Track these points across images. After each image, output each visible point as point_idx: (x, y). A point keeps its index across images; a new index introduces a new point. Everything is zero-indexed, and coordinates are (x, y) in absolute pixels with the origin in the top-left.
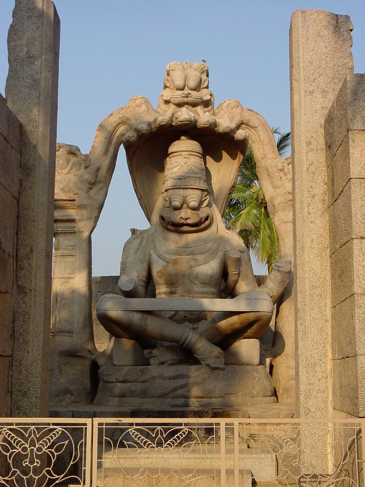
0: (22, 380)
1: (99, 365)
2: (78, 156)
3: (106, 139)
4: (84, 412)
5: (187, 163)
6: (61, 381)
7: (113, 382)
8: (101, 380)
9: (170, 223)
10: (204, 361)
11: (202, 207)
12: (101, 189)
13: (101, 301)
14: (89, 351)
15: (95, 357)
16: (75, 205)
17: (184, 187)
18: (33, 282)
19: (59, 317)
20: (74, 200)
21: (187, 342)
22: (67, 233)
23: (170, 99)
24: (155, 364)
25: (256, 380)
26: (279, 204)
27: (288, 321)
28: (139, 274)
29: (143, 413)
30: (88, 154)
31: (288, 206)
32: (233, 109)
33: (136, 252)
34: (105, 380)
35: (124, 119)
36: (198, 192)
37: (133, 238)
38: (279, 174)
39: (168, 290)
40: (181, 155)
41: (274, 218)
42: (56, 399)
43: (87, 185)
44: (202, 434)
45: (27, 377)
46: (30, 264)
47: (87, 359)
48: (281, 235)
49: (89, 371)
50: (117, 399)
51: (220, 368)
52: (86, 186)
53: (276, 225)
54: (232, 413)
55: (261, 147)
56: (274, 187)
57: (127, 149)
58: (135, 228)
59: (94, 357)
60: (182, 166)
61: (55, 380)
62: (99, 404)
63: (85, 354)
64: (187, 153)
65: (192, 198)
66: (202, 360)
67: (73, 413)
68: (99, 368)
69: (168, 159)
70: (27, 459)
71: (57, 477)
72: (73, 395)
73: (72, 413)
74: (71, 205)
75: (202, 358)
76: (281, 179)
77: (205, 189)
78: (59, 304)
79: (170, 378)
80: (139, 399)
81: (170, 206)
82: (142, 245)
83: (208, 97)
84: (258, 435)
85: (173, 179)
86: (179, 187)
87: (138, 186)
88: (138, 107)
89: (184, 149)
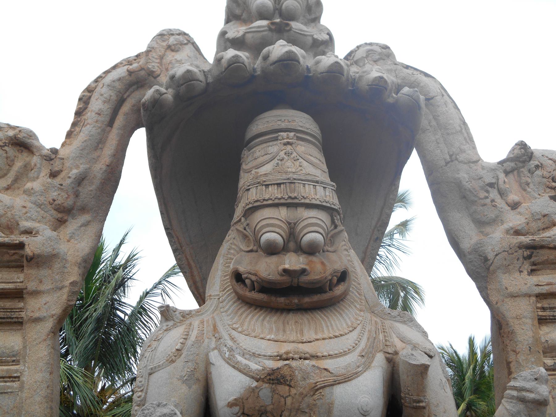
2: (35, 150)
9: (255, 283)
11: (330, 249)
12: (86, 224)
16: (23, 256)
17: (290, 201)
20: (21, 246)
23: (244, 35)
26: (497, 255)
30: (58, 147)
31: (518, 259)
35: (143, 73)
36: (323, 216)
37: (165, 328)
38: (487, 195)
40: (277, 140)
41: (487, 288)
43: (54, 212)
48: (508, 324)
52: (52, 216)
53: (494, 303)
60: (281, 160)
64: (292, 134)
69: (245, 152)
74: (13, 258)
76: (493, 203)
77: (336, 208)
81: (255, 248)
82: (189, 342)
85: (263, 185)
88: (173, 51)
89: (283, 125)
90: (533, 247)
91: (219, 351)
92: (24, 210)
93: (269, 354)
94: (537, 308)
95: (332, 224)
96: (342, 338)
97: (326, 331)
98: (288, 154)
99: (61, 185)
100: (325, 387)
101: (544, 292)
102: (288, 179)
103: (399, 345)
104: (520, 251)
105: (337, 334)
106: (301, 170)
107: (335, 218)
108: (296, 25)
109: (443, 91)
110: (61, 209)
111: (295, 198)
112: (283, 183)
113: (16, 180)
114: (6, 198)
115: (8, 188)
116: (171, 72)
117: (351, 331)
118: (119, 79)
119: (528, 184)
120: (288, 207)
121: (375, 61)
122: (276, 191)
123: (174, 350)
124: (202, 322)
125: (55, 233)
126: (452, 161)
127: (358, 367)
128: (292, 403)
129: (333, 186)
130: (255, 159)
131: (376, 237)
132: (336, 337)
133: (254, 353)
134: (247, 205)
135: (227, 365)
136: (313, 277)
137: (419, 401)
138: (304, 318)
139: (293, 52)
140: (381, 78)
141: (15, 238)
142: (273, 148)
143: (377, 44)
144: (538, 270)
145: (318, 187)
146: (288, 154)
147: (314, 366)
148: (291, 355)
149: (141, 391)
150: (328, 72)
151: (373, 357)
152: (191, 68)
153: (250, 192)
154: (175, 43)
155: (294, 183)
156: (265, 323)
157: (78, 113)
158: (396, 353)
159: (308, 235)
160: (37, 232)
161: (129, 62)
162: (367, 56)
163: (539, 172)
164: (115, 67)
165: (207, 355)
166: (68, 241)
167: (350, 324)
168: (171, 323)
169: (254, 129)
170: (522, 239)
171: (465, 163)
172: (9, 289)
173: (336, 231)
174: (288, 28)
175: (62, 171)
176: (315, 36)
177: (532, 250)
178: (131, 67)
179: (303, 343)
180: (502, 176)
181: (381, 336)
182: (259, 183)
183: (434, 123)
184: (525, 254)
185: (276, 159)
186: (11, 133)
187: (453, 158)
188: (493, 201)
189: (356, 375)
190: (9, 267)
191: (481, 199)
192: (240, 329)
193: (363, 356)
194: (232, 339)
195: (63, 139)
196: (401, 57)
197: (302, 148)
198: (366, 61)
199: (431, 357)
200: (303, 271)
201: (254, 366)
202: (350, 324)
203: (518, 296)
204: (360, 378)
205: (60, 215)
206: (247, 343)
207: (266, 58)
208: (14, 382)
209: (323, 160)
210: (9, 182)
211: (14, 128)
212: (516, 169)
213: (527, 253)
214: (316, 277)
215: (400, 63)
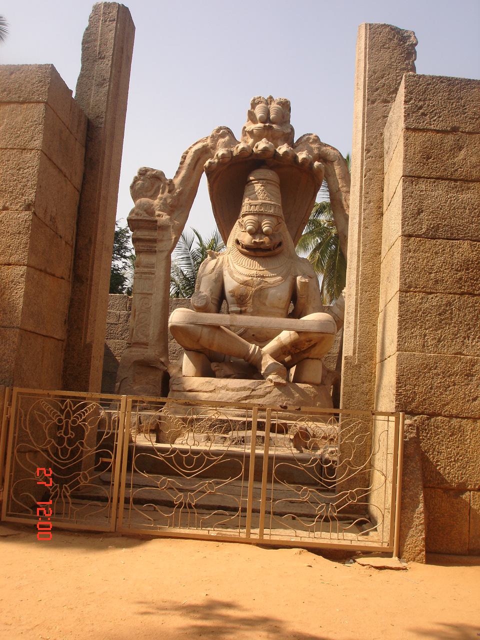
0: (74, 364)
4: (150, 415)
6: (134, 388)
11: (276, 233)
14: (162, 363)
18: (90, 272)
19: (136, 330)
20: (156, 221)
21: (252, 359)
28: (212, 293)
30: (172, 178)
34: (174, 389)
36: (274, 219)
39: (239, 309)
45: (78, 362)
46: (88, 255)
47: (160, 370)
49: (161, 381)
54: (290, 426)
57: (207, 175)
59: (166, 368)
61: (129, 387)
65: (264, 224)
68: (170, 379)
69: (246, 186)
70: (62, 430)
71: (89, 449)
78: (136, 318)
79: (233, 390)
83: (289, 131)
87: (217, 213)
103: (299, 272)
110: (171, 206)
111: (262, 211)
113: (154, 193)
114: (151, 200)
118: (199, 149)
131: (303, 222)
137: (303, 296)
151: (287, 277)
157: (182, 163)
160: (162, 217)
164: (197, 143)
207: (257, 147)
209: (279, 191)
211: (154, 170)
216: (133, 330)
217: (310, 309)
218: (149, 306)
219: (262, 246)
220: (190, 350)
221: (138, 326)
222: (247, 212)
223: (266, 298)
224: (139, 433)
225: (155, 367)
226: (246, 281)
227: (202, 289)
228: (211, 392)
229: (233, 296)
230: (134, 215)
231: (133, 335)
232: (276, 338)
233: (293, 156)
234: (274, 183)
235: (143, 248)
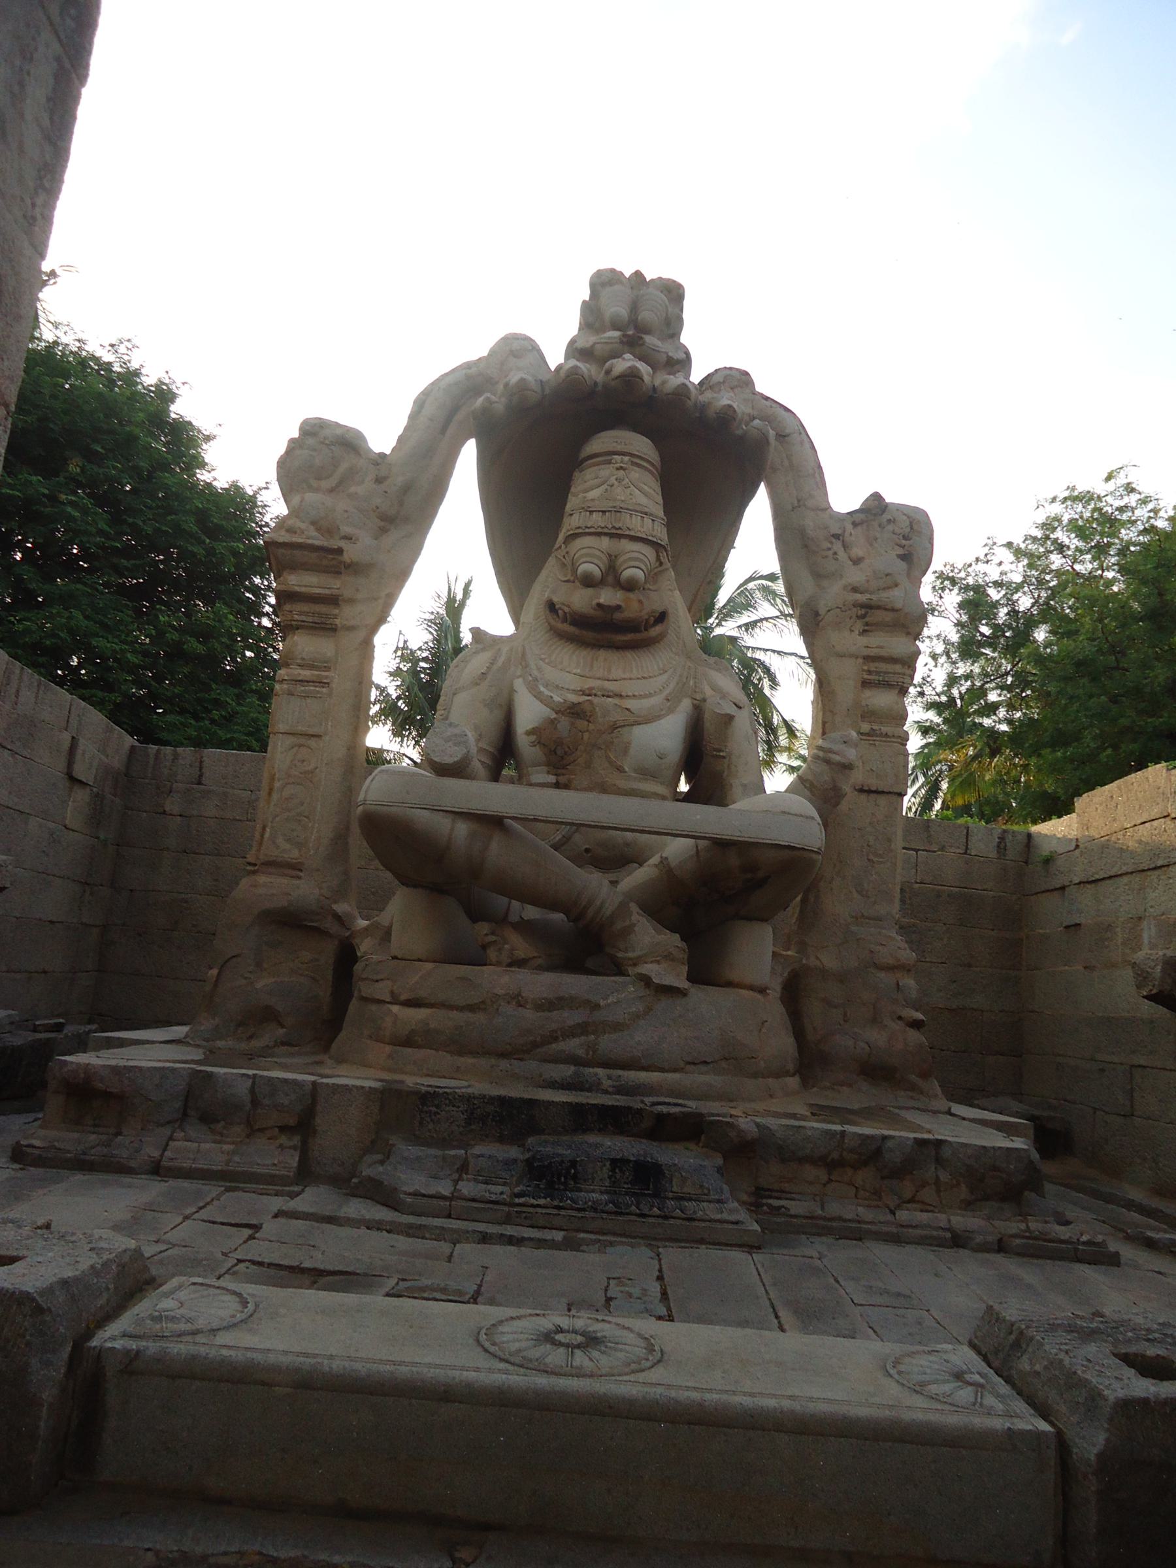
1: (359, 954)
2: (362, 453)
3: (431, 420)
4: (286, 1081)
5: (623, 480)
6: (259, 985)
7: (384, 1002)
8: (356, 994)
10: (635, 965)
11: (651, 587)
13: (372, 781)
14: (338, 918)
15: (350, 935)
16: (341, 562)
19: (272, 827)
20: (340, 551)
21: (591, 912)
22: (316, 628)
23: (593, 346)
24: (498, 964)
25: (764, 1030)
26: (829, 611)
27: (831, 889)
28: (480, 735)
29: (455, 1099)
30: (388, 452)
31: (851, 618)
32: (736, 390)
33: (478, 681)
34: (364, 995)
36: (649, 552)
38: (829, 546)
39: (552, 779)
42: (239, 1032)
44: (625, 1183)
50: (388, 1049)
51: (679, 988)
54: (712, 1122)
55: (792, 481)
56: (818, 576)
58: (482, 628)
59: (347, 934)
60: (612, 486)
61: (244, 982)
62: (340, 1060)
63: (329, 925)
66: (630, 962)
67: (254, 1083)
69: (576, 474)
72: (283, 1026)
73: (251, 1080)
75: (630, 959)
76: (835, 556)
78: (275, 796)
80: (448, 1055)
81: (572, 578)
82: (495, 667)
84: (782, 1191)
86: (600, 530)
88: (515, 356)
90: (868, 607)
91: (524, 679)
92: (346, 515)
93: (572, 688)
94: (863, 670)
95: (657, 561)
96: (651, 679)
97: (634, 671)
98: (619, 480)
99: (386, 492)
100: (624, 726)
101: (872, 654)
102: (615, 507)
103: (708, 692)
104: (855, 609)
105: (645, 676)
106: (631, 499)
107: (661, 555)
108: (649, 339)
109: (801, 428)
111: (620, 528)
112: (609, 511)
115: (331, 490)
116: (507, 379)
117: (661, 674)
119: (876, 539)
120: (610, 538)
121: (732, 388)
122: (600, 519)
123: (480, 673)
124: (511, 650)
125: (376, 542)
126: (799, 507)
127: (662, 710)
128: (589, 738)
129: (663, 520)
130: (585, 482)
132: (644, 678)
133: (557, 686)
134: (568, 531)
135: (530, 695)
136: (627, 614)
137: (720, 751)
138: (613, 656)
139: (636, 368)
140: (730, 406)
141: (335, 543)
142: (605, 471)
143: (737, 369)
144: (871, 631)
145: (645, 519)
146: (619, 480)
147: (616, 705)
148: (594, 691)
149: (444, 710)
150: (674, 393)
151: (680, 701)
152: (524, 376)
153: (573, 517)
154: (518, 348)
155: (620, 512)
156: (574, 657)
158: (704, 700)
159: (629, 570)
160: (357, 539)
161: (468, 365)
162: (724, 382)
163: (890, 527)
165: (512, 685)
166: (389, 551)
167: (661, 666)
168: (480, 646)
169: (587, 449)
170: (860, 595)
171: (813, 510)
172: (325, 594)
173: (659, 569)
174: (641, 342)
175: (388, 477)
176: (670, 354)
177: (867, 610)
178: (469, 371)
179: (608, 680)
180: (849, 527)
181: (691, 683)
182: (583, 508)
183: (786, 463)
184: (860, 612)
185: (605, 485)
186: (339, 432)
187: (800, 504)
188: (835, 553)
189: (659, 717)
190: (328, 573)
191: (824, 550)
192: (547, 661)
193: (668, 700)
194: (539, 669)
195: (394, 444)
196: (760, 387)
197: (635, 474)
198: (722, 388)
199: (740, 708)
200: (618, 608)
201: (557, 699)
202: (661, 666)
203: (844, 656)
204: (662, 721)
205: (382, 524)
206: (551, 674)
208: (323, 687)
209: (659, 490)
210: (334, 485)
212: (866, 521)
213: (863, 611)
214: (631, 615)
215: (759, 393)
216: (264, 829)
217: (737, 790)
218: (310, 768)
219: (618, 616)
220: (415, 886)
221: (277, 819)
222: (579, 528)
223: (626, 751)
224: (248, 1136)
225: (317, 930)
226: (574, 705)
227: (454, 717)
228: (471, 1008)
229: (533, 744)
230: (283, 533)
231: (265, 839)
232: (655, 860)
233: (695, 404)
234: (645, 464)
235: (304, 618)
